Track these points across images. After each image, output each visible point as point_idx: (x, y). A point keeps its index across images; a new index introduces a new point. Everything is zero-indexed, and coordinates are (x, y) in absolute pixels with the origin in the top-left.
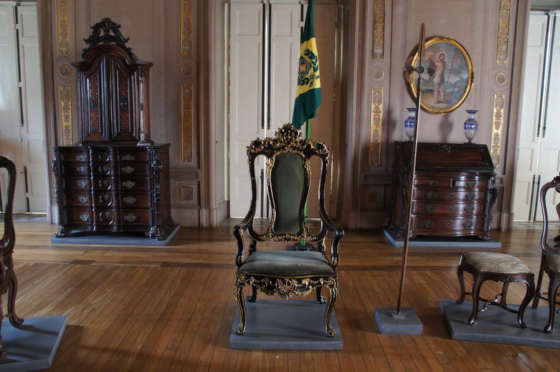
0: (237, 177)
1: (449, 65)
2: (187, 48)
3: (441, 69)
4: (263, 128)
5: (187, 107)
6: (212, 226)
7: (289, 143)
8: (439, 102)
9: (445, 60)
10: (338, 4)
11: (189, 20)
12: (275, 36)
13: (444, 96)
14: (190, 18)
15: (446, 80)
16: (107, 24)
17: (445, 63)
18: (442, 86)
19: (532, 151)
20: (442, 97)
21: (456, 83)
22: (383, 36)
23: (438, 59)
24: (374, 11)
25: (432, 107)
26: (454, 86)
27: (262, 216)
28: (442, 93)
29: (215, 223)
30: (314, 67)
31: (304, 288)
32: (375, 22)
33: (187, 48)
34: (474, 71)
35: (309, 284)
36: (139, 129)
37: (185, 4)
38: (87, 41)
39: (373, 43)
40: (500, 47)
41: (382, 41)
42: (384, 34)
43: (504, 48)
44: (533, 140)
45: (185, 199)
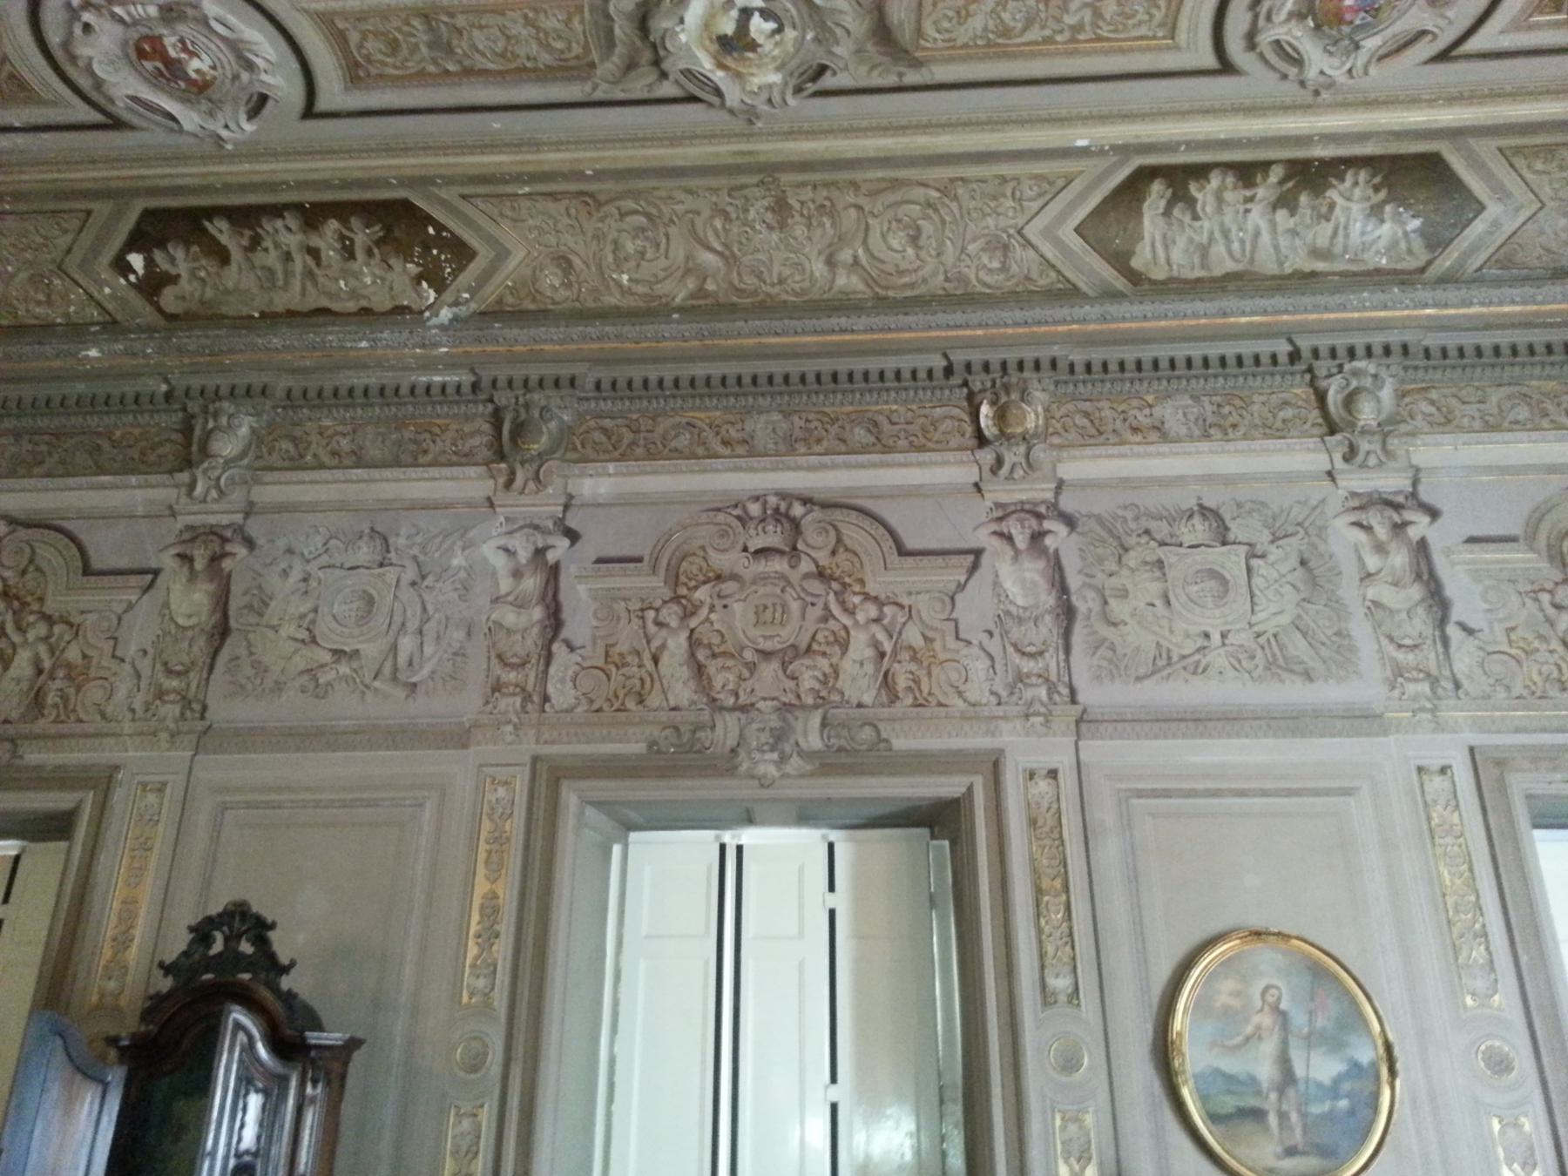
2: (481, 983)
10: (933, 837)
11: (496, 897)
14: (500, 893)
22: (1071, 935)
24: (1032, 860)
32: (1039, 891)
33: (481, 983)
34: (1391, 1037)
37: (489, 852)
38: (167, 969)
39: (1042, 956)
40: (1464, 953)
41: (1068, 948)
42: (1071, 929)
43: (1479, 953)
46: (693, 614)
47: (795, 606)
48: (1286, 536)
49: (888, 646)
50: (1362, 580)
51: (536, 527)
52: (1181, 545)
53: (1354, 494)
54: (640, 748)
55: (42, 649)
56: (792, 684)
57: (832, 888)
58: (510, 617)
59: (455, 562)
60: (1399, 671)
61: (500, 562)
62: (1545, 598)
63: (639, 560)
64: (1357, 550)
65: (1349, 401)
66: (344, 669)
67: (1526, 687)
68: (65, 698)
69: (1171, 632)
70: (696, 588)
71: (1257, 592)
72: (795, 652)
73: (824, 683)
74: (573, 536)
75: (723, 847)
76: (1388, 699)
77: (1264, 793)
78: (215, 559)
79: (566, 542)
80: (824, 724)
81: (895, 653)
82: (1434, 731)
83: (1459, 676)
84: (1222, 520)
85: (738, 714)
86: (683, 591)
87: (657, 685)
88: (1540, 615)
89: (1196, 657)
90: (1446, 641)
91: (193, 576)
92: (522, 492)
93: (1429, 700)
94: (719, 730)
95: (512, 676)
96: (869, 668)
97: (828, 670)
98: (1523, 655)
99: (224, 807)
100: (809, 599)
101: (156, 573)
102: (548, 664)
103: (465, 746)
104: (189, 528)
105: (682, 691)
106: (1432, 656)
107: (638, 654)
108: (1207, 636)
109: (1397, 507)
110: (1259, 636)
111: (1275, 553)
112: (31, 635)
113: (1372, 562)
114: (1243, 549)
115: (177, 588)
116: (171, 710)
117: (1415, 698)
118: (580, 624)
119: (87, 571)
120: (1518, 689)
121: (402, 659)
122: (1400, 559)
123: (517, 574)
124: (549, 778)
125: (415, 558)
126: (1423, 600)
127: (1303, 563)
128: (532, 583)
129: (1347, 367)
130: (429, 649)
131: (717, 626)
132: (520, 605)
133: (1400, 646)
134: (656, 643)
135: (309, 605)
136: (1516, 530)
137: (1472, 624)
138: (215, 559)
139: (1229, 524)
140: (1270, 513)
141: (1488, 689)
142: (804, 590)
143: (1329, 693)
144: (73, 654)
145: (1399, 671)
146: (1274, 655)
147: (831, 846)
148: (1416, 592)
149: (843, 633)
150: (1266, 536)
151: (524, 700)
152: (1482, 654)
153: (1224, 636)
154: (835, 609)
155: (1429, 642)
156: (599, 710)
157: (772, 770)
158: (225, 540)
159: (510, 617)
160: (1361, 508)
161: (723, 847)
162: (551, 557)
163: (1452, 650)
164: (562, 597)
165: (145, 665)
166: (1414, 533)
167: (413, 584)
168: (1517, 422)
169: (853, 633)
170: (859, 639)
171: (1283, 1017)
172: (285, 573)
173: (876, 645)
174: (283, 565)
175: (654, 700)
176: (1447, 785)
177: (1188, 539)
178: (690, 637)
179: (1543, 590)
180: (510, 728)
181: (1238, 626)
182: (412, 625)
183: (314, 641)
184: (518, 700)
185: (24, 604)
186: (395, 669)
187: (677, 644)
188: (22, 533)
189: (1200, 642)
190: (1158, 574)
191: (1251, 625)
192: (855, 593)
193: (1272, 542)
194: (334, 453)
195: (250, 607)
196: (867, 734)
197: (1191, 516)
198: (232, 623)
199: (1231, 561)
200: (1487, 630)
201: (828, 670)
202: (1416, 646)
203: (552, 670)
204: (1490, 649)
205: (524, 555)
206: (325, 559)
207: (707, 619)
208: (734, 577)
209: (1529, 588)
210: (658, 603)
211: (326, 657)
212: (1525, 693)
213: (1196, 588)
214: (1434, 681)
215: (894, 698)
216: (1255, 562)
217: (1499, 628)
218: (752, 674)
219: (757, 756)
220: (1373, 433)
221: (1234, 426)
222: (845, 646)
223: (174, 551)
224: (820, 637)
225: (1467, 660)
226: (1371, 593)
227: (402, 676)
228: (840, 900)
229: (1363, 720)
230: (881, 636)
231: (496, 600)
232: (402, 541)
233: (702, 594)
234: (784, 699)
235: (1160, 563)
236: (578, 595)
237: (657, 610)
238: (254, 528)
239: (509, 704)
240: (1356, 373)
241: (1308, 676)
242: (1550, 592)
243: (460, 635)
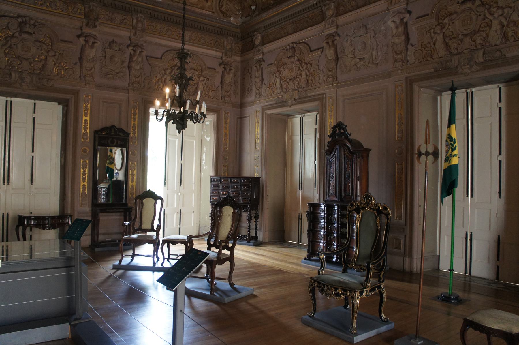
0: (446, 237)
2: (400, 135)
4: (468, 196)
5: (400, 179)
6: (405, 270)
7: (368, 205)
11: (401, 114)
12: (477, 118)
16: (339, 126)
27: (465, 273)
29: (415, 269)
30: (452, 148)
31: (338, 295)
33: (400, 135)
35: (342, 293)
36: (356, 194)
45: (395, 248)
46: (444, 27)
47: (474, 17)
49: (505, 23)
51: (400, 13)
54: (432, 70)
55: (306, 70)
56: (474, 43)
57: (500, 101)
58: (397, 40)
59: (382, 28)
61: (392, 25)
63: (428, 15)
66: (362, 63)
68: (312, 81)
70: (444, 19)
72: (475, 32)
73: (484, 40)
74: (410, 12)
75: (467, 93)
78: (333, 41)
79: (408, 15)
80: (484, 53)
81: (508, 24)
85: (458, 56)
86: (440, 21)
87: (435, 52)
91: (330, 47)
92: (395, 4)
94: (453, 62)
95: (399, 57)
96: (499, 32)
97: (485, 36)
99: (344, 100)
100: (479, 14)
101: (323, 48)
102: (407, 52)
103: (390, 77)
104: (327, 35)
105: (442, 52)
107: (430, 43)
112: (304, 68)
115: (327, 50)
116: (331, 79)
118: (414, 39)
119: (311, 51)
121: (374, 57)
123: (397, 28)
124: (410, 82)
125: (373, 30)
128: (401, 29)
130: (379, 54)
131: (451, 30)
132: (399, 37)
134: (435, 39)
135: (353, 48)
138: (333, 41)
142: (477, 11)
144: (312, 71)
147: (500, 89)
149: (490, 22)
151: (402, 63)
154: (487, 15)
156: (421, 62)
157: (468, 71)
158: (334, 36)
159: (397, 40)
161: (467, 93)
162: (405, 20)
164: (409, 31)
165: (324, 70)
167: (374, 37)
169: (493, 21)
170: (495, 23)
172: (347, 41)
173: (501, 23)
174: (346, 39)
175: (435, 56)
178: (443, 35)
180: (400, 71)
182: (375, 48)
183: (355, 57)
184: (401, 63)
185: (302, 61)
186: (373, 60)
187: (440, 38)
188: (298, 45)
192: (494, 7)
194: (352, 7)
195: (341, 52)
196: (498, 54)
198: (339, 57)
201: (485, 36)
203: (408, 53)
205: (398, 22)
206: (354, 36)
207: (448, 28)
208: (456, 13)
210: (434, 27)
211: (358, 60)
215: (507, 40)
218: (462, 42)
219: (463, 67)
222: (490, 26)
223: (325, 42)
224: (482, 26)
227: (374, 62)
228: (503, 105)
230: (503, 20)
231: (393, 37)
232: (370, 26)
233: (446, 21)
234: (472, 48)
236: (413, 29)
237: (434, 29)
238: (339, 32)
239: (399, 64)
243: (386, 48)
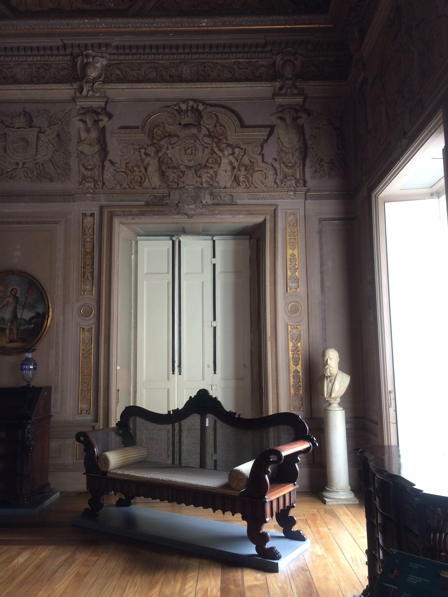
1: (22, 300)
3: (13, 305)
8: (11, 341)
9: (17, 295)
13: (17, 334)
15: (19, 316)
17: (17, 298)
18: (15, 323)
19: (168, 391)
20: (15, 336)
21: (33, 318)
23: (9, 294)
25: (4, 347)
26: (30, 321)
28: (15, 330)
44: (168, 378)
48: (53, 125)
50: (78, 143)
52: (14, 127)
53: (82, 108)
60: (84, 178)
62: (143, 151)
64: (79, 131)
65: (85, 67)
67: (128, 185)
69: (5, 162)
71: (39, 147)
76: (78, 188)
77: (27, 223)
82: (92, 201)
83: (105, 180)
84: (31, 117)
88: (139, 158)
89: (12, 172)
90: (103, 167)
93: (92, 189)
98: (129, 173)
106: (97, 174)
108: (17, 164)
109: (97, 114)
110: (36, 164)
111: (49, 131)
113: (84, 135)
114: (37, 130)
117: (88, 188)
120: (125, 185)
122: (94, 134)
126: (99, 151)
127: (58, 135)
129: (84, 53)
133: (86, 169)
136: (140, 124)
137: (114, 161)
139: (34, 119)
140: (50, 115)
141: (114, 185)
143: (57, 186)
145: (84, 178)
146: (40, 172)
148: (96, 148)
150: (46, 125)
152: (115, 172)
153: (24, 164)
155: (97, 167)
160: (84, 114)
163: (104, 171)
166: (101, 124)
168: (150, 79)
171: (17, 299)
176: (92, 220)
177: (17, 125)
179: (143, 148)
181: (29, 160)
189: (15, 166)
190: (4, 139)
191: (34, 160)
193: (48, 127)
197: (20, 116)
199: (32, 134)
200: (119, 163)
202: (92, 169)
204: (118, 171)
209: (138, 147)
212: (127, 187)
213: (17, 145)
214: (96, 182)
216: (41, 135)
217: (123, 163)
220: (90, 82)
221: (43, 77)
225: (109, 174)
226: (80, 148)
229: (67, 196)
235: (5, 135)
240: (87, 56)
241: (51, 180)
242: (145, 149)
